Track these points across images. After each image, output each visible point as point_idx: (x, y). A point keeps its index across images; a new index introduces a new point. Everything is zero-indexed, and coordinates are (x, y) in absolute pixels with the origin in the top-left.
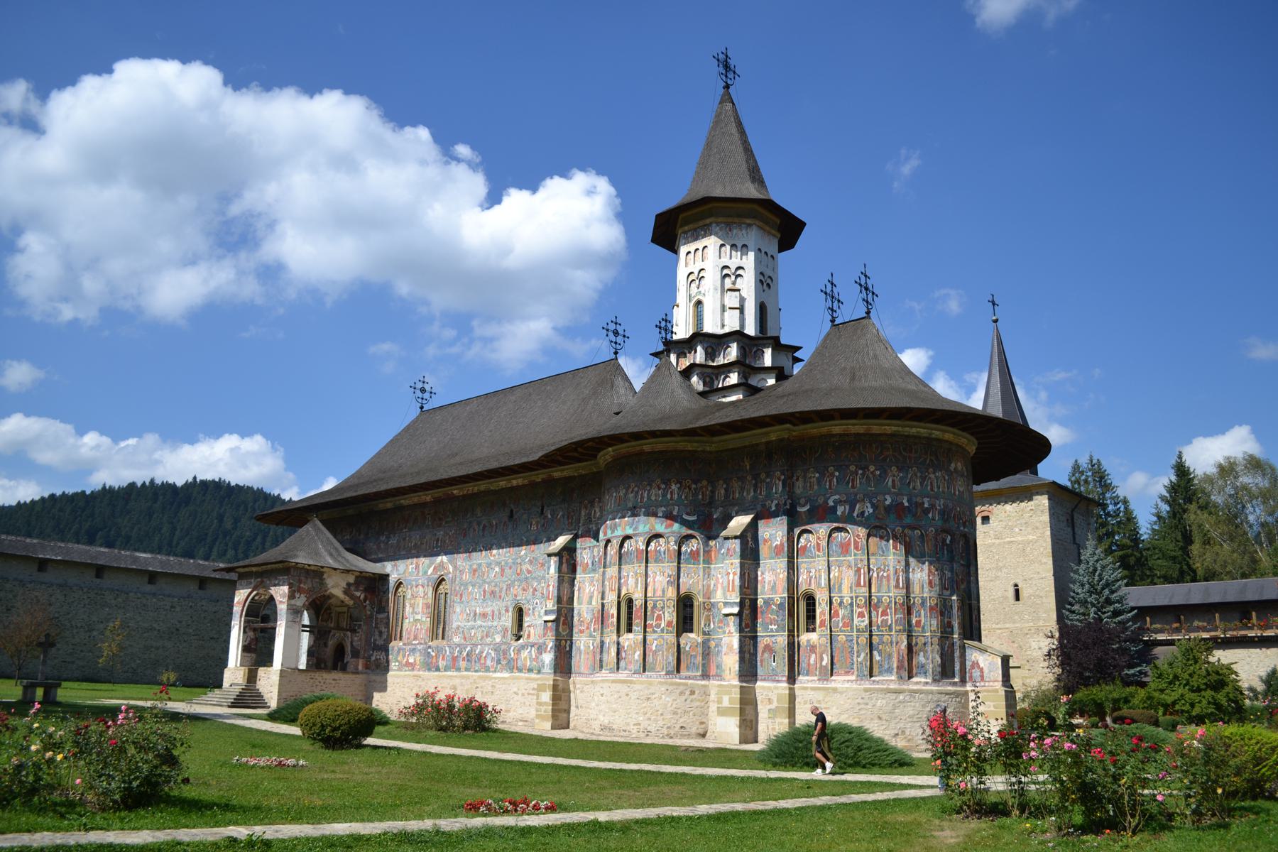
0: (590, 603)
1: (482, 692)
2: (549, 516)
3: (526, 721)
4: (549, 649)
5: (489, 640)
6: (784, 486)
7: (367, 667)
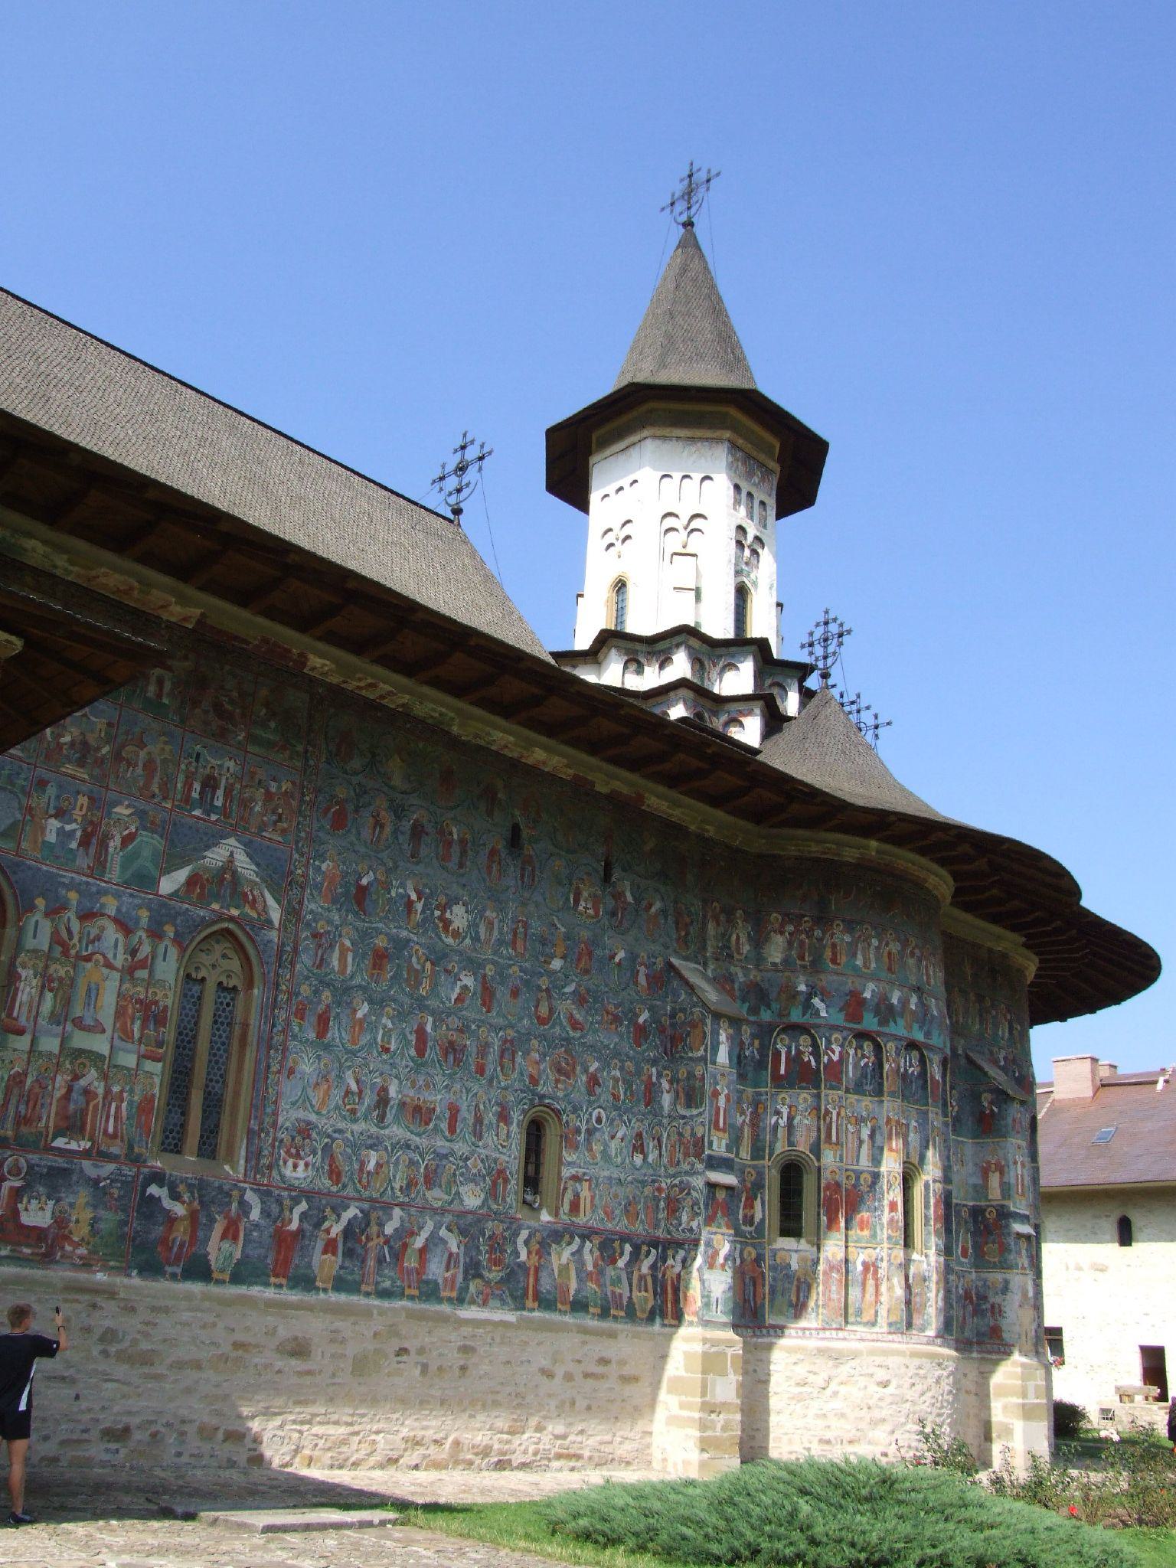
1: (425, 1368)
2: (630, 899)
4: (721, 1260)
5: (436, 1196)
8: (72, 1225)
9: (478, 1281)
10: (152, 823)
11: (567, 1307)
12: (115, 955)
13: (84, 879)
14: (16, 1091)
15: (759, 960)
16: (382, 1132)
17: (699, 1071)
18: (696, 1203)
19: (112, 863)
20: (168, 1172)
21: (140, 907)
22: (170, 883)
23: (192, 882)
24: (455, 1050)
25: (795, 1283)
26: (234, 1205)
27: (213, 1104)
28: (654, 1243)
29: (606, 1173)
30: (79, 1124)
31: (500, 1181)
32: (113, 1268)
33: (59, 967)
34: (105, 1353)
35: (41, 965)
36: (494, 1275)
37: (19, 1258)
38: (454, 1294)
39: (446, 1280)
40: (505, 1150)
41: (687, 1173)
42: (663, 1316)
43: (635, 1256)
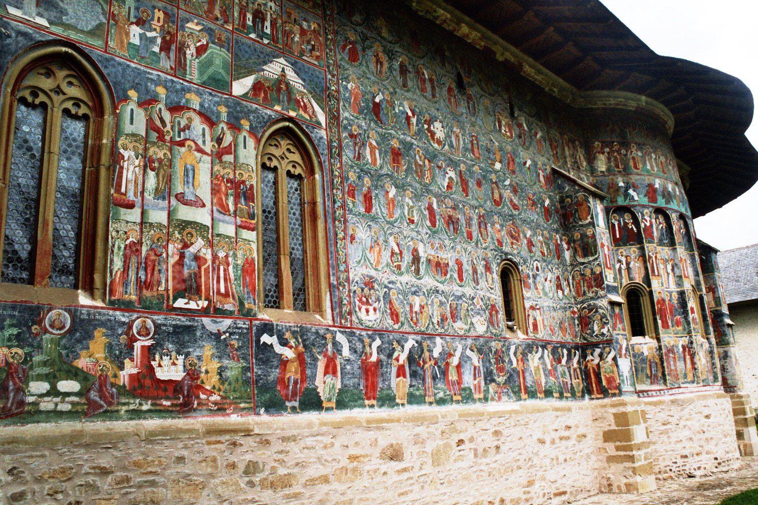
1: (476, 450)
2: (526, 128)
3: (564, 493)
4: (624, 352)
5: (459, 326)
8: (203, 375)
9: (493, 384)
10: (219, 39)
11: (542, 395)
12: (204, 142)
13: (169, 77)
14: (134, 259)
15: (593, 170)
16: (419, 281)
17: (589, 232)
18: (603, 316)
19: (190, 67)
20: (275, 323)
21: (218, 104)
22: (241, 87)
23: (257, 87)
24: (453, 222)
25: (648, 363)
26: (330, 347)
27: (300, 267)
28: (577, 347)
29: (546, 304)
30: (194, 286)
31: (494, 312)
32: (244, 409)
33: (157, 150)
34: (251, 484)
35: (141, 147)
36: (501, 379)
37: (160, 411)
38: (482, 396)
39: (475, 385)
40: (492, 291)
41: (592, 298)
42: (590, 392)
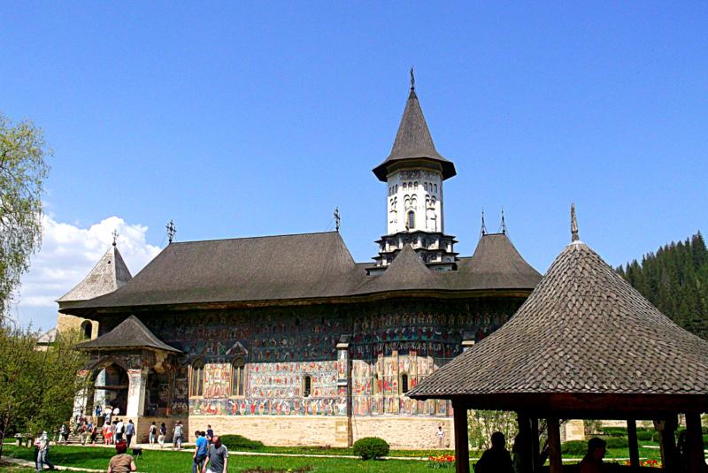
0: (364, 375)
5: (283, 396)
6: (491, 320)
7: (171, 413)
43: (334, 401)
